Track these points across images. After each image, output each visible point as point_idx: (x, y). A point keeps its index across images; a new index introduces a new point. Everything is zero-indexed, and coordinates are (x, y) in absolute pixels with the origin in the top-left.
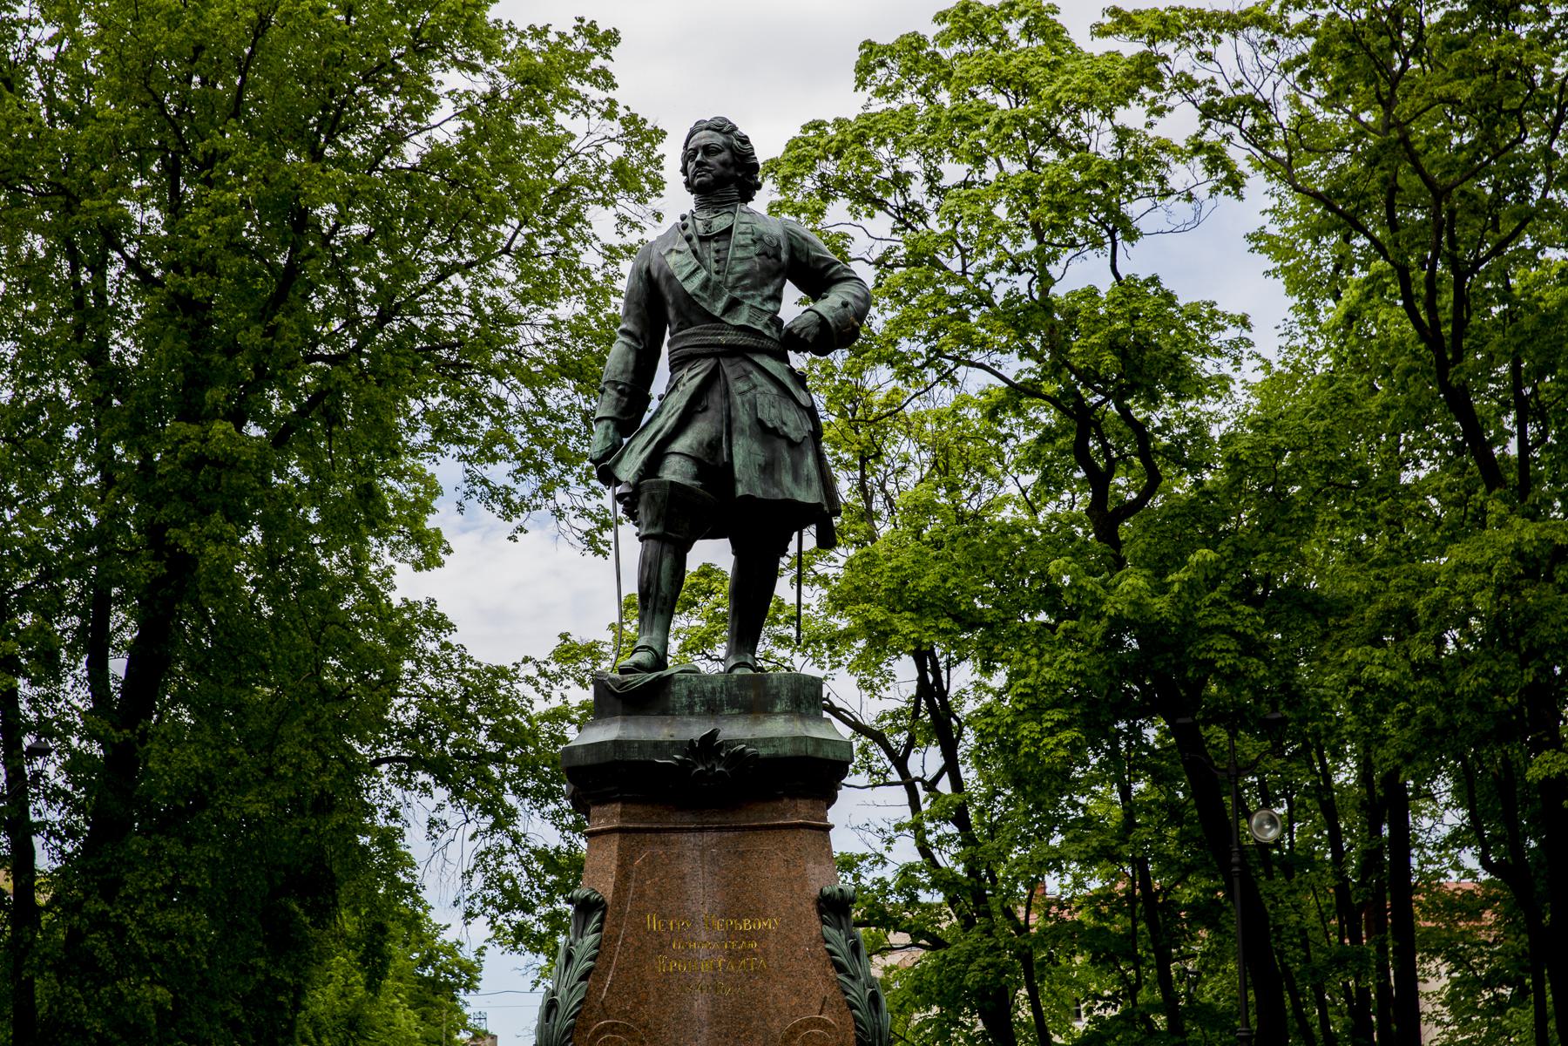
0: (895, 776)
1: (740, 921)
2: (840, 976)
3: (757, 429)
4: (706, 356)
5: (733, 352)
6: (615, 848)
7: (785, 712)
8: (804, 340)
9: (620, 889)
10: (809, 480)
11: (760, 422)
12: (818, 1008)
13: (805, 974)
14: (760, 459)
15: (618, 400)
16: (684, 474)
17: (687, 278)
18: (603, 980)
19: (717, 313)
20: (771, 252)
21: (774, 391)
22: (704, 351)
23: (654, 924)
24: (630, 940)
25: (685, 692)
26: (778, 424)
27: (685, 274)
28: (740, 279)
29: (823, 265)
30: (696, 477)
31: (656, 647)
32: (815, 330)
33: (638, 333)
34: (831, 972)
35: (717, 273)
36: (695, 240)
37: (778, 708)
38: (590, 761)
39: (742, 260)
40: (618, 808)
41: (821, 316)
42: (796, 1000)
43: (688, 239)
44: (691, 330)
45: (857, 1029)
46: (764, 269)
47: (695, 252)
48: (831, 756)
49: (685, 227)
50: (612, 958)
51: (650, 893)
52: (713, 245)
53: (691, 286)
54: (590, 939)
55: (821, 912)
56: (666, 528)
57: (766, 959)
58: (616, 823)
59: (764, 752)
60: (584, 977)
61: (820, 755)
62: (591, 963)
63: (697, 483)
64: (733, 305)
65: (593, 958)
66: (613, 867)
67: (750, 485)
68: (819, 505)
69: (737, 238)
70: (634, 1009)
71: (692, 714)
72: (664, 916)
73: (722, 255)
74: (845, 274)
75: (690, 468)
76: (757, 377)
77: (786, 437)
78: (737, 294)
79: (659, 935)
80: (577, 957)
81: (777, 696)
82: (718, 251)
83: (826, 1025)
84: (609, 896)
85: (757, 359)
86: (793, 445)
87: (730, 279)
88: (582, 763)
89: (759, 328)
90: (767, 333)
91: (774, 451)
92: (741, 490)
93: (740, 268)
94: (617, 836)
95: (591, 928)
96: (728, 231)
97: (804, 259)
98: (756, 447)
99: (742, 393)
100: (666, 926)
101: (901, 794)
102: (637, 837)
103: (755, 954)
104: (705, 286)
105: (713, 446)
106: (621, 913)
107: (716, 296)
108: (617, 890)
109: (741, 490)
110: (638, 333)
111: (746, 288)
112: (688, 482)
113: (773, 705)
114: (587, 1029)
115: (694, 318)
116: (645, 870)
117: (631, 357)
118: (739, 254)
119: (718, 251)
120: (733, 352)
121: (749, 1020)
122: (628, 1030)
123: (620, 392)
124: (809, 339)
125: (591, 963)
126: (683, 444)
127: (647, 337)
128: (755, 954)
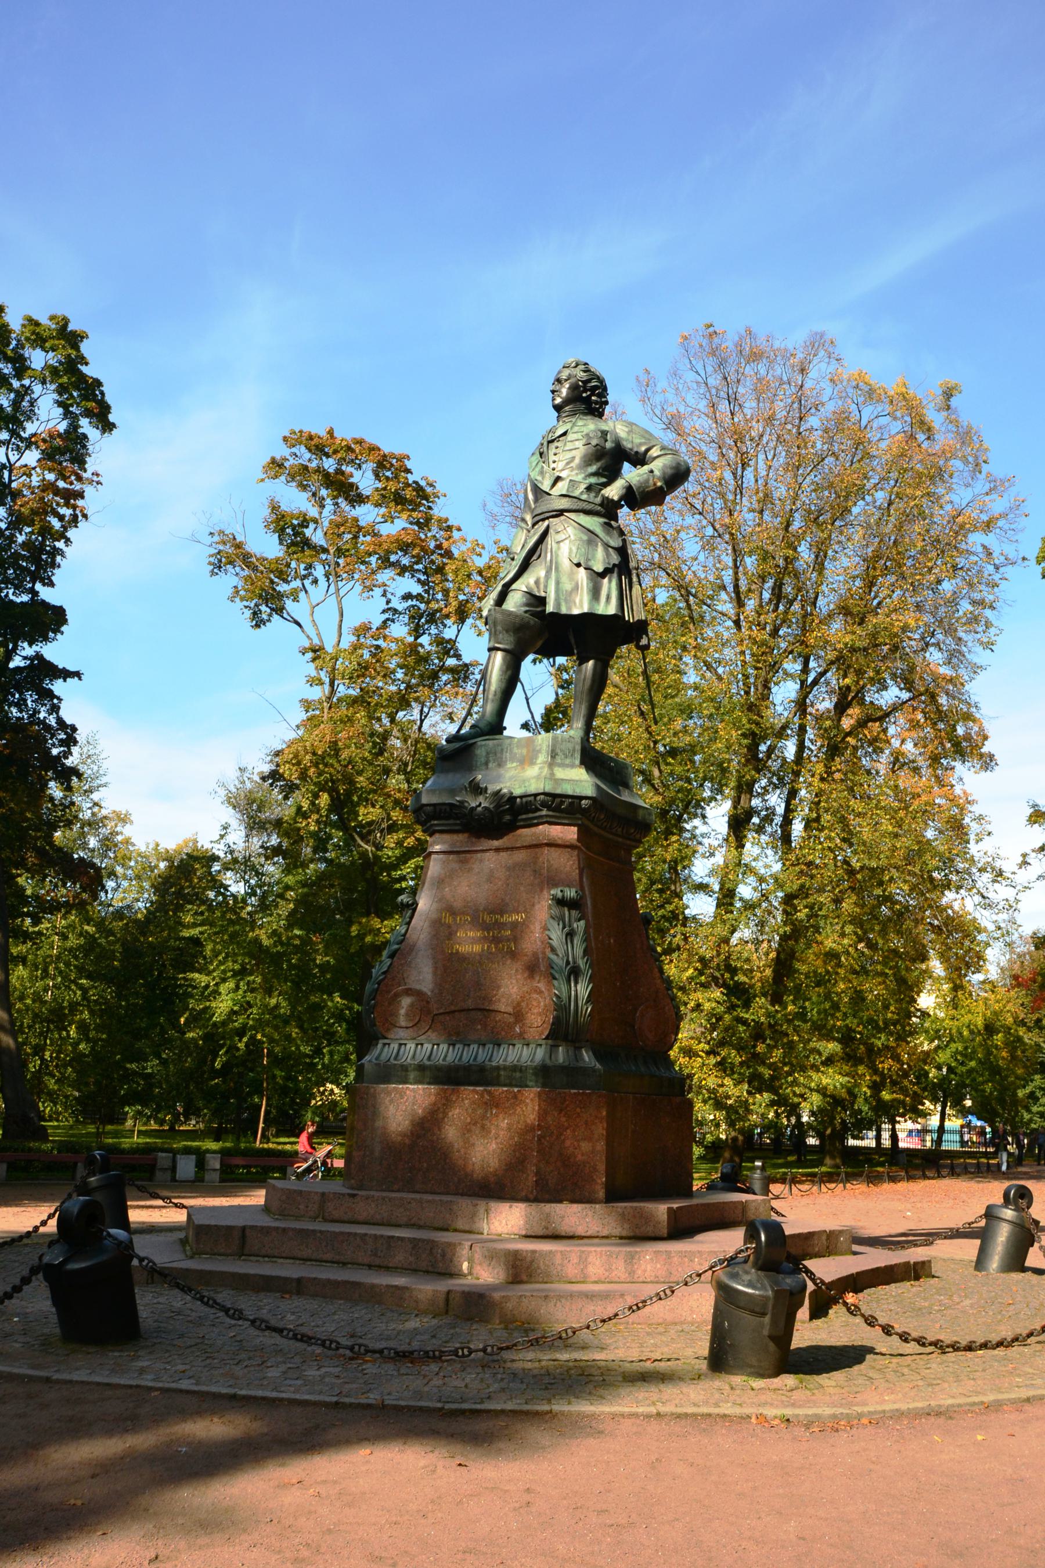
4: (543, 520)
8: (612, 500)
10: (608, 598)
21: (585, 538)
22: (542, 517)
25: (484, 754)
28: (568, 463)
29: (643, 449)
48: (570, 792)
52: (556, 444)
61: (559, 791)
64: (558, 479)
67: (558, 604)
78: (563, 474)
81: (539, 751)
82: (557, 448)
89: (576, 493)
92: (550, 608)
96: (565, 434)
97: (629, 446)
114: (388, 992)
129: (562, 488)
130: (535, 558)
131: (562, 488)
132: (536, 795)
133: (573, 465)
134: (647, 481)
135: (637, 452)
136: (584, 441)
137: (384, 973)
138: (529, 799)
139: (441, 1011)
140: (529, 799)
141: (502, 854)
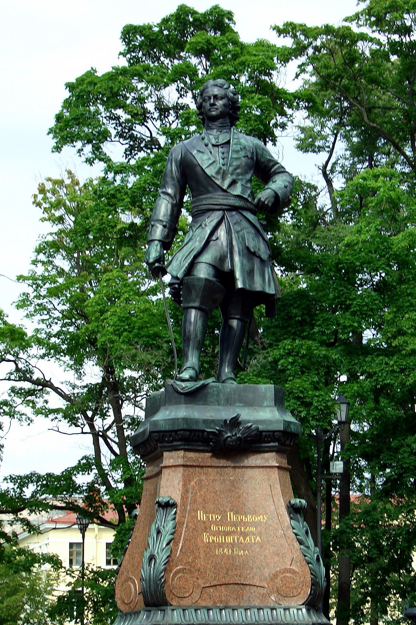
0: (87, 429)
1: (246, 517)
2: (302, 547)
3: (246, 251)
4: (219, 210)
5: (233, 208)
6: (180, 475)
7: (269, 406)
9: (184, 497)
11: (248, 248)
12: (289, 563)
13: (282, 546)
14: (247, 268)
15: (163, 230)
16: (209, 274)
17: (207, 167)
18: (178, 545)
19: (225, 187)
20: (250, 156)
23: (201, 516)
24: (190, 524)
25: (216, 393)
26: (257, 250)
27: (207, 165)
28: (235, 169)
29: (271, 164)
30: (215, 276)
31: (196, 368)
32: (273, 200)
33: (173, 195)
34: (297, 544)
35: (223, 165)
36: (210, 146)
37: (265, 404)
38: (167, 428)
39: (236, 159)
40: (182, 453)
41: (275, 192)
42: (277, 558)
43: (206, 145)
44: (209, 195)
45: (312, 574)
46: (247, 164)
47: (211, 153)
49: (203, 139)
50: (181, 534)
51: (200, 500)
52: (221, 150)
53: (210, 172)
54: (171, 524)
55: (289, 514)
56: (202, 303)
57: (260, 537)
58: (180, 462)
59: (261, 427)
60: (168, 544)
61: (289, 430)
62: (172, 536)
63: (214, 279)
64: (233, 183)
65: (172, 534)
66: (181, 485)
68: (273, 295)
69: (233, 147)
70: (193, 561)
71: (219, 405)
72: (206, 513)
73: (225, 155)
74: (282, 170)
75: (211, 270)
76: (245, 223)
77: (259, 257)
79: (204, 522)
80: (163, 533)
81: (265, 397)
83: (294, 572)
84: (178, 501)
85: (245, 213)
86: (262, 260)
87: (231, 169)
88: (163, 429)
90: (250, 199)
91: (253, 265)
93: (235, 163)
94: (181, 469)
95: (170, 517)
96: (228, 142)
97: (262, 160)
98: (245, 261)
99: (238, 232)
100: (208, 518)
101: (90, 437)
102: (191, 470)
103: (254, 534)
104: (218, 173)
105: (222, 259)
106: (185, 510)
107: (223, 179)
108: (182, 498)
109: (240, 285)
110: (173, 195)
111: (238, 175)
112: (211, 278)
113: (263, 402)
114: (171, 571)
115: (210, 189)
116: (196, 488)
117: (170, 206)
118: (235, 156)
119: (223, 153)
120: (233, 208)
121: (252, 568)
122: (191, 572)
123: (165, 226)
124: (270, 204)
125: (172, 536)
126: (207, 257)
127: (178, 197)
128: (254, 534)
129: (237, 190)
130: (214, 238)
131: (237, 190)
132: (274, 432)
133: (238, 171)
134: (286, 193)
135: (266, 166)
136: (242, 154)
137: (168, 557)
138: (268, 433)
139: (208, 585)
140: (268, 433)
141: (237, 470)
